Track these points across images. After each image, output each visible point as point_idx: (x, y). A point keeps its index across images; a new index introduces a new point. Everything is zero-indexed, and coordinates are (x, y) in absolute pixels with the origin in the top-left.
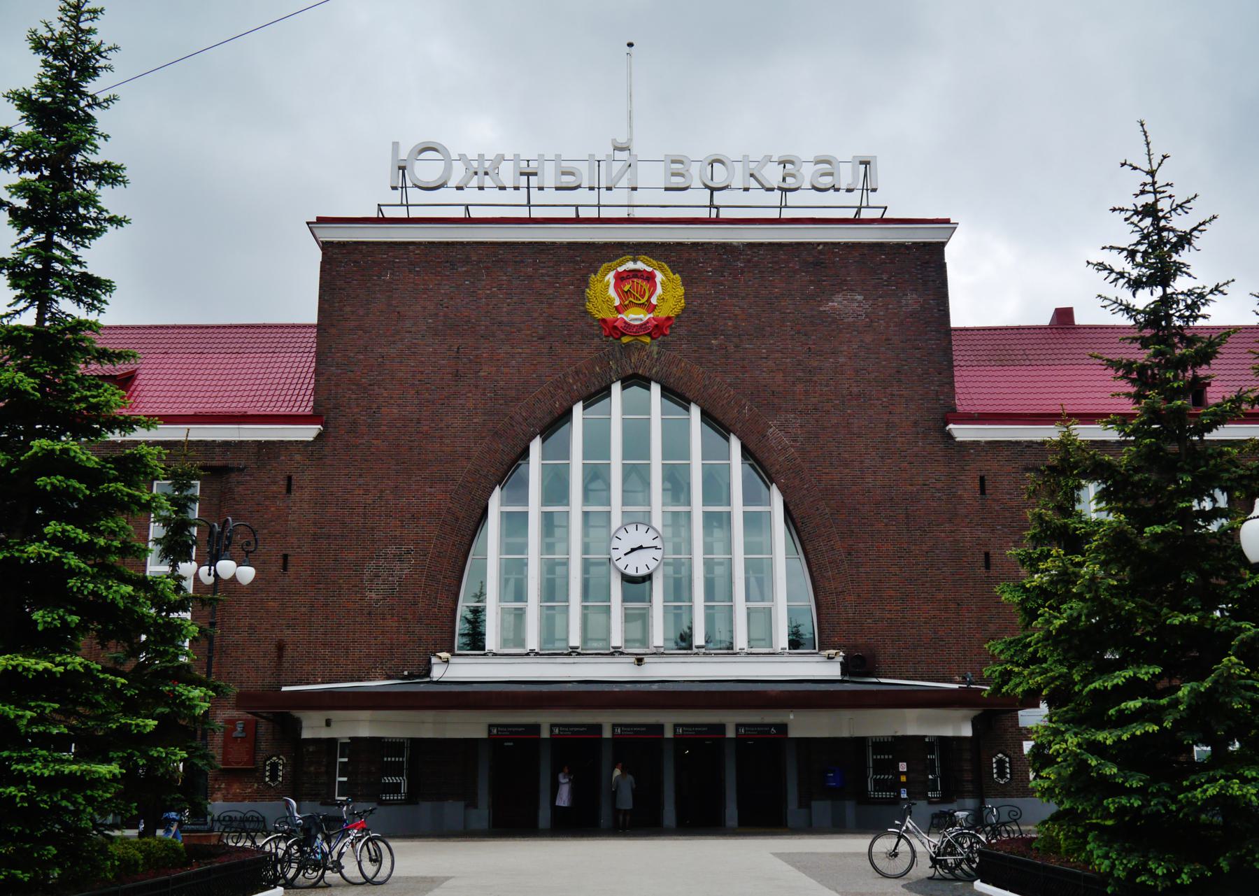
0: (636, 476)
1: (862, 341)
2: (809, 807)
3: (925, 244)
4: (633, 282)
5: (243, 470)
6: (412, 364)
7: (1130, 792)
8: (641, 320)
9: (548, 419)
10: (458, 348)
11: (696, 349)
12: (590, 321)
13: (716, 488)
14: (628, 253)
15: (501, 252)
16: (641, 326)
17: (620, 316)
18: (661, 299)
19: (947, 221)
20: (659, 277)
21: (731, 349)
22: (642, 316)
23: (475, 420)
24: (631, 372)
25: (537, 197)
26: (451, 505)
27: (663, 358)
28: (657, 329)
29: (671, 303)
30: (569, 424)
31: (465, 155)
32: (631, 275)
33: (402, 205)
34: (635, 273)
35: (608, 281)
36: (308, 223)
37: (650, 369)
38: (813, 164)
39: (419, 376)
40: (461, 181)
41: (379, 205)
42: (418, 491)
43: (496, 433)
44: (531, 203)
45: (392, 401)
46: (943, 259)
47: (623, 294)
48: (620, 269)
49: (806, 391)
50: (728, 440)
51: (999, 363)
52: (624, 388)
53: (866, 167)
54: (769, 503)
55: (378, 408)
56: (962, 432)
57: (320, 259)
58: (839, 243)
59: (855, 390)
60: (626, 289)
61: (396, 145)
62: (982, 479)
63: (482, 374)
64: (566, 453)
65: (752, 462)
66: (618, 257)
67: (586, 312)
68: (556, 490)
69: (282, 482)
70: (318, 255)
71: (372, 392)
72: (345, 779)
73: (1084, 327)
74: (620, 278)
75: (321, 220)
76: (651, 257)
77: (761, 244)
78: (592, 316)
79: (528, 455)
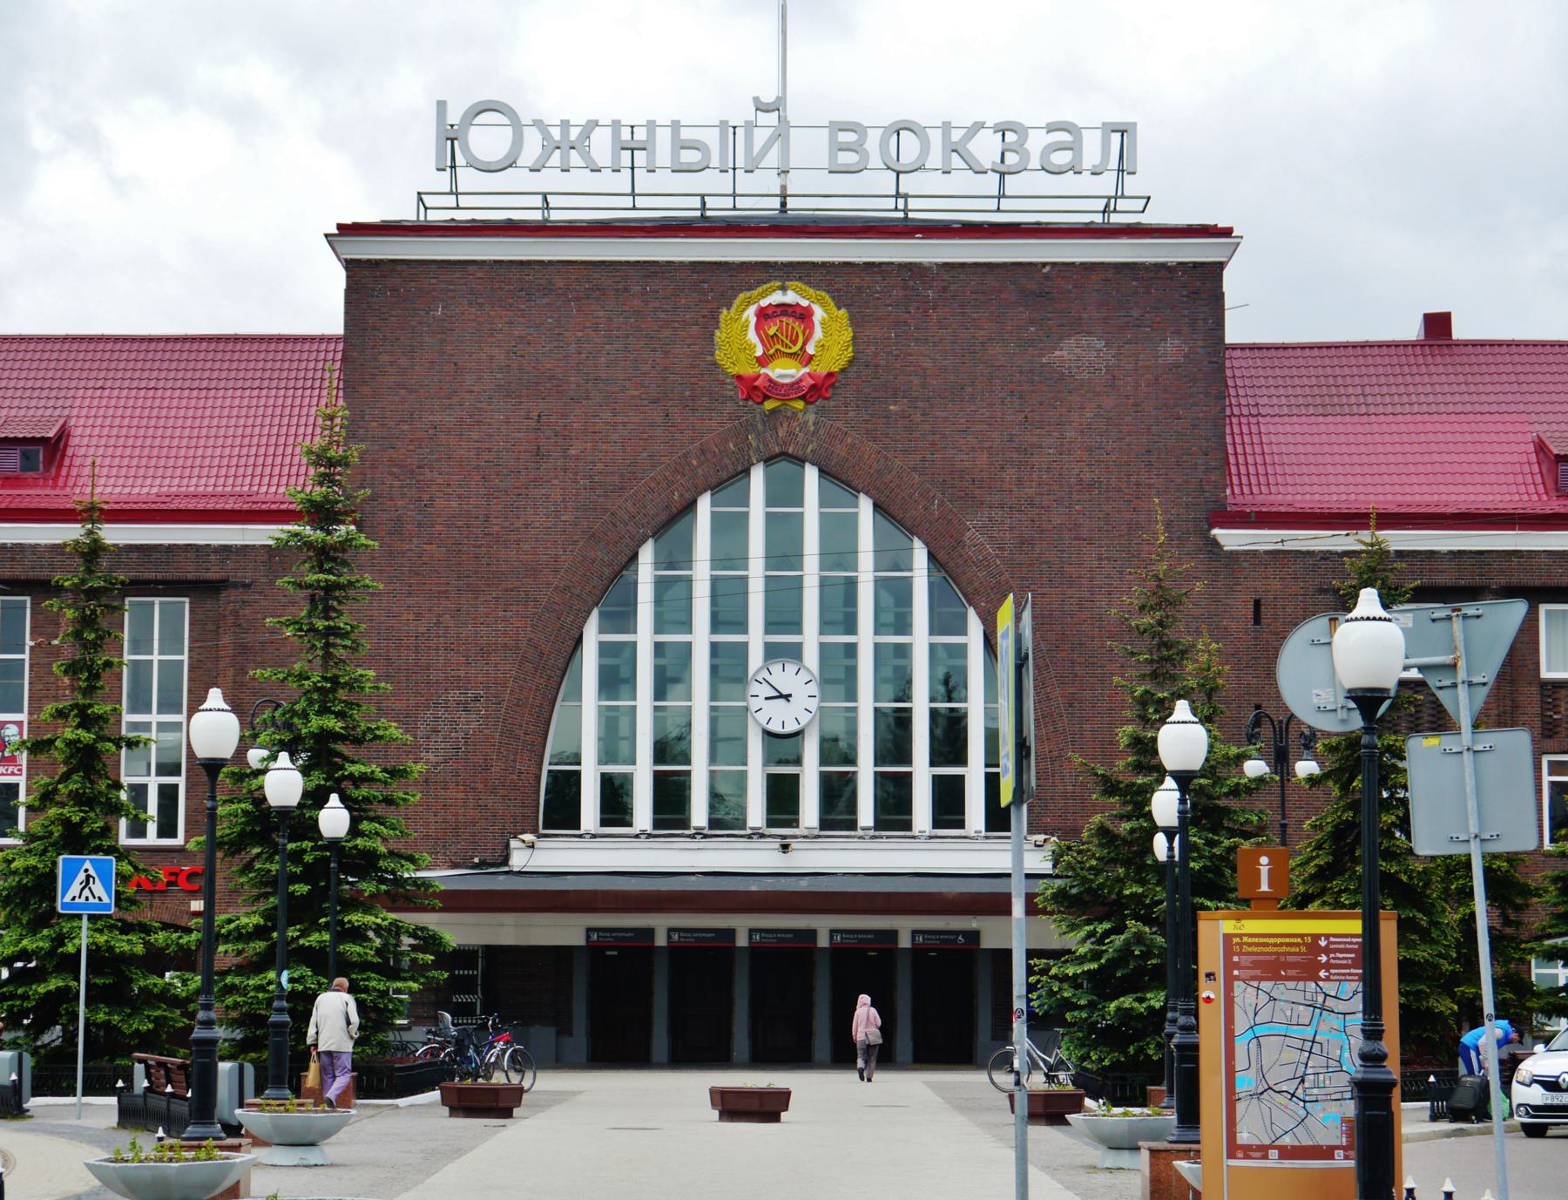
0: (783, 617)
1: (1099, 407)
3: (1196, 265)
4: (781, 321)
5: (249, 586)
6: (476, 438)
7: (1081, 1008)
8: (793, 376)
9: (664, 517)
10: (539, 416)
12: (721, 377)
13: (894, 599)
14: (776, 278)
16: (793, 384)
17: (763, 371)
19: (1227, 232)
20: (819, 314)
21: (918, 417)
22: (792, 371)
23: (563, 518)
24: (777, 450)
25: (644, 182)
26: (533, 636)
27: (821, 432)
28: (816, 390)
29: (835, 352)
31: (541, 121)
32: (779, 311)
33: (451, 193)
34: (784, 309)
35: (747, 320)
36: (326, 236)
37: (805, 447)
38: (1044, 131)
39: (485, 456)
40: (537, 160)
41: (419, 193)
42: (487, 615)
43: (593, 536)
44: (636, 192)
45: (450, 490)
46: (1221, 287)
47: (767, 340)
48: (764, 303)
51: (1320, 410)
53: (1122, 136)
55: (431, 499)
56: (1231, 539)
58: (1073, 263)
59: (1087, 476)
60: (771, 332)
61: (442, 106)
62: (1257, 603)
63: (572, 452)
66: (760, 283)
68: (673, 612)
71: (421, 477)
74: (764, 315)
75: (344, 229)
76: (809, 283)
77: (963, 265)
78: (725, 373)
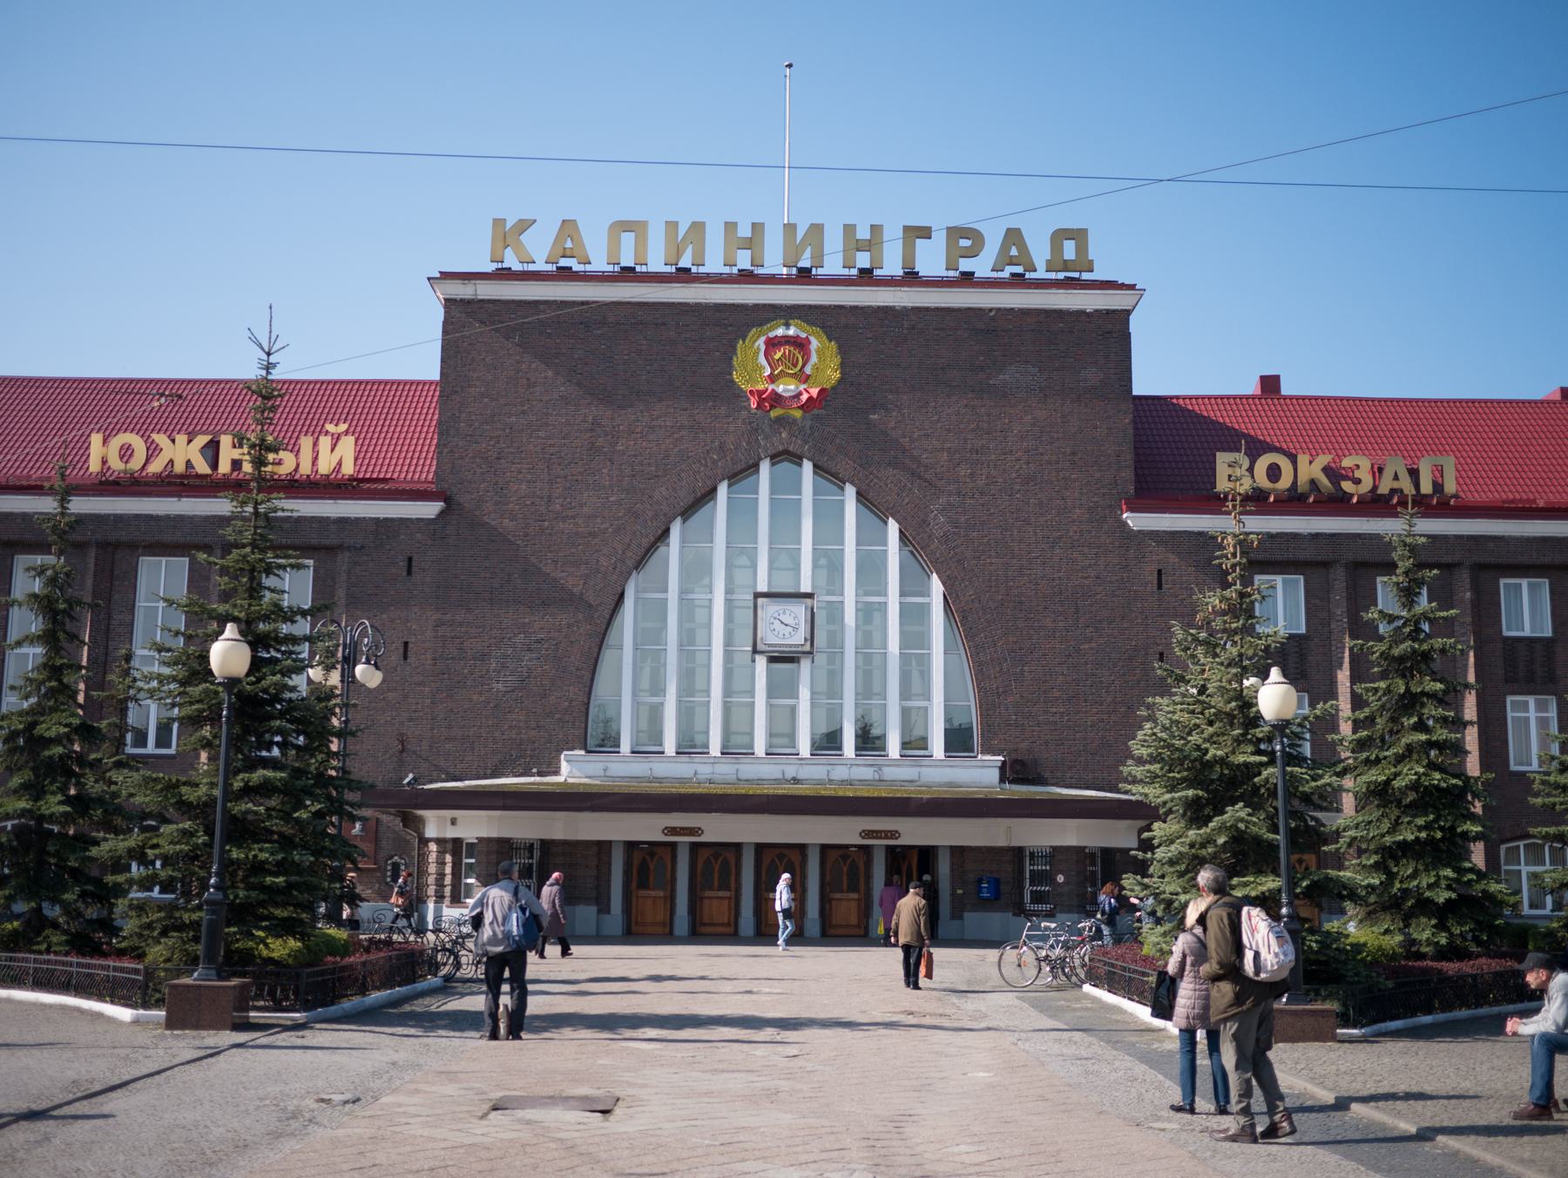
2: (961, 918)
9: (691, 499)
11: (852, 423)
12: (737, 392)
15: (640, 313)
18: (816, 368)
19: (1132, 287)
20: (815, 343)
22: (792, 387)
24: (781, 448)
27: (816, 435)
30: (712, 502)
34: (787, 340)
35: (759, 349)
36: (429, 279)
48: (772, 335)
49: (972, 475)
50: (886, 523)
52: (773, 464)
54: (926, 593)
57: (442, 319)
65: (911, 548)
67: (732, 381)
69: (401, 564)
70: (439, 314)
73: (1291, 398)
74: (772, 344)
75: (446, 276)
79: (668, 536)
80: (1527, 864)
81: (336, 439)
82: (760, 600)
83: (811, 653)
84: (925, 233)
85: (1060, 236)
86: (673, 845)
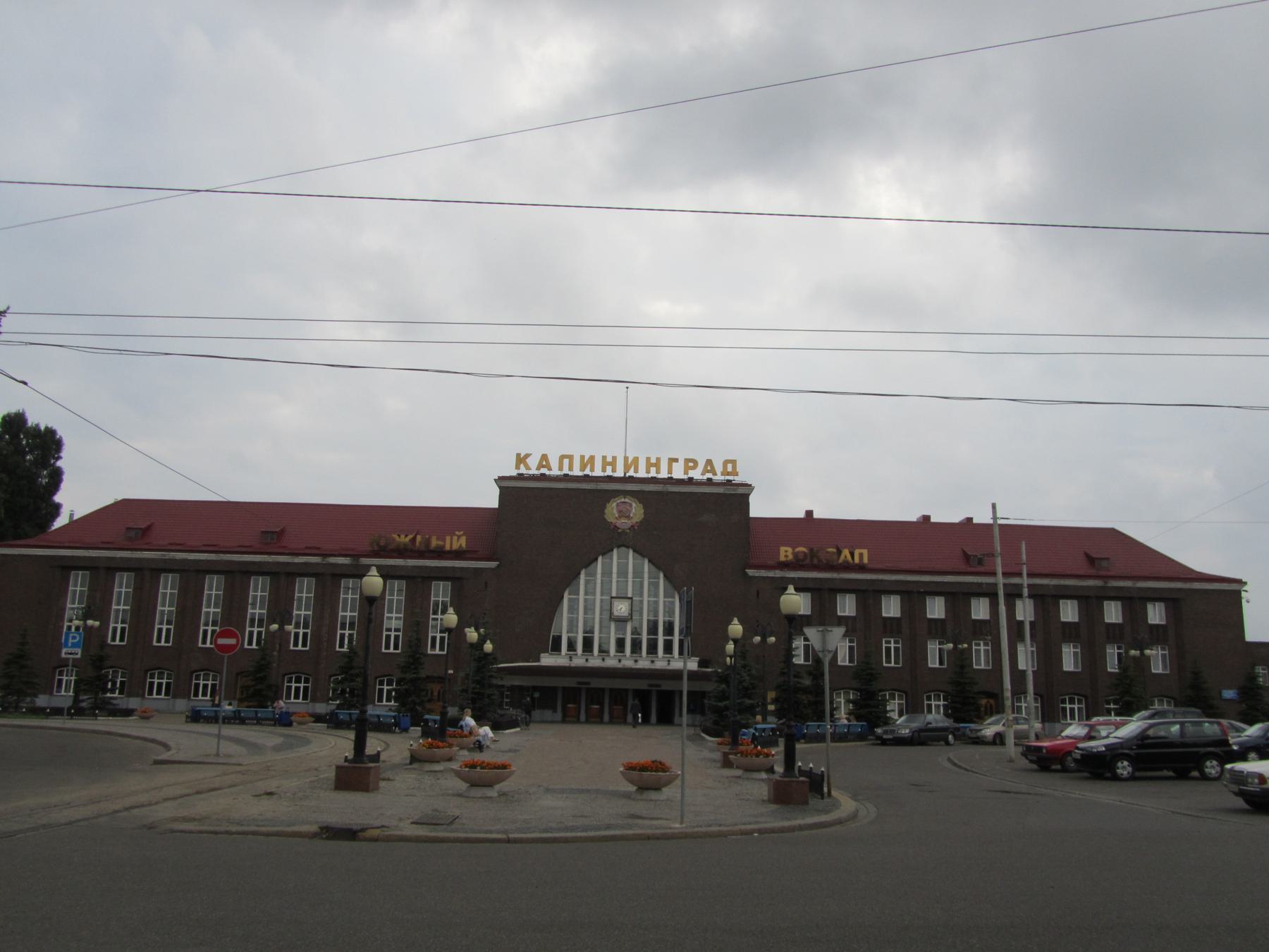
18: (635, 514)
19: (750, 485)
20: (634, 505)
47: (620, 512)
56: (751, 572)
62: (758, 592)
64: (594, 574)
66: (618, 496)
72: (508, 700)
74: (618, 505)
80: (934, 701)
81: (459, 537)
82: (613, 600)
83: (631, 618)
84: (676, 460)
85: (726, 462)
86: (580, 689)
